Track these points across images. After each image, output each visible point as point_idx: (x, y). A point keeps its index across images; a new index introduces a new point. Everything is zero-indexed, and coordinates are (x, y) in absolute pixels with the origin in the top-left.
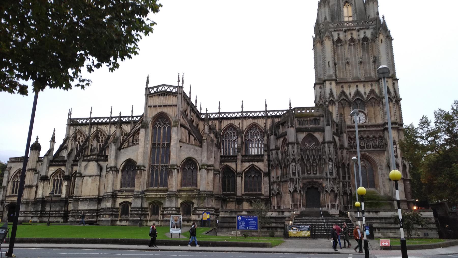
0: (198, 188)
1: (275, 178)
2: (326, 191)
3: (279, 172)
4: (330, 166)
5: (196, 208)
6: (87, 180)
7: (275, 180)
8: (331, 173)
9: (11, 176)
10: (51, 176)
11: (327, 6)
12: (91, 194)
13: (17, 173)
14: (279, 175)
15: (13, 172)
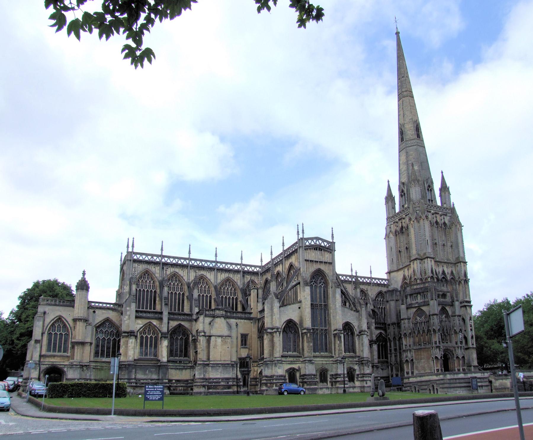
0: (358, 354)
1: (408, 345)
2: (457, 357)
3: (412, 339)
4: (461, 336)
5: (358, 375)
6: (216, 341)
7: (408, 348)
8: (461, 342)
9: (46, 325)
10: (138, 331)
11: (417, 185)
12: (223, 359)
13: (55, 322)
14: (411, 343)
15: (49, 319)
